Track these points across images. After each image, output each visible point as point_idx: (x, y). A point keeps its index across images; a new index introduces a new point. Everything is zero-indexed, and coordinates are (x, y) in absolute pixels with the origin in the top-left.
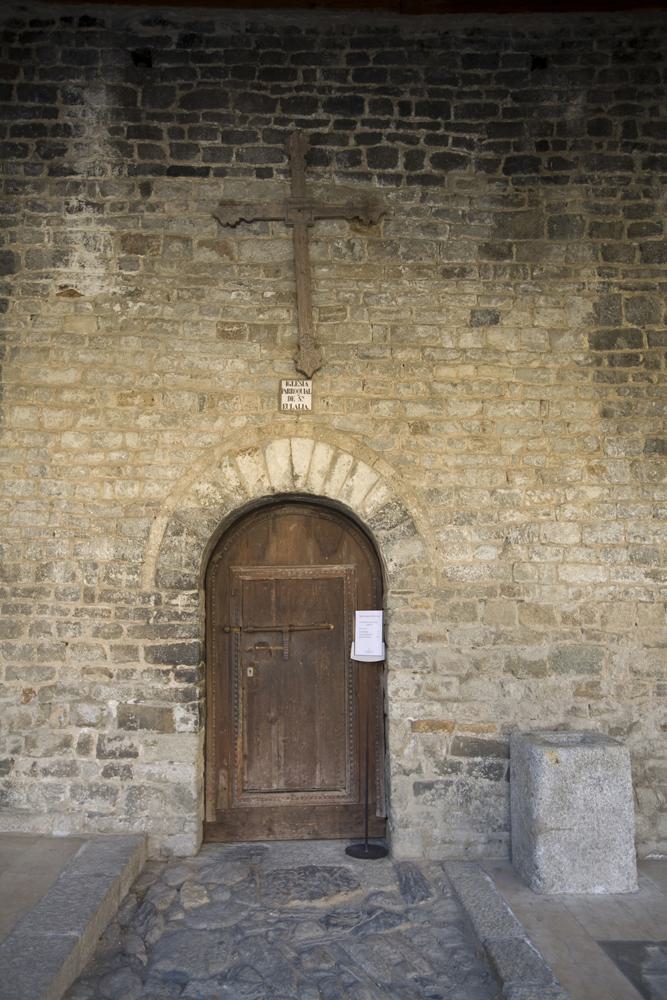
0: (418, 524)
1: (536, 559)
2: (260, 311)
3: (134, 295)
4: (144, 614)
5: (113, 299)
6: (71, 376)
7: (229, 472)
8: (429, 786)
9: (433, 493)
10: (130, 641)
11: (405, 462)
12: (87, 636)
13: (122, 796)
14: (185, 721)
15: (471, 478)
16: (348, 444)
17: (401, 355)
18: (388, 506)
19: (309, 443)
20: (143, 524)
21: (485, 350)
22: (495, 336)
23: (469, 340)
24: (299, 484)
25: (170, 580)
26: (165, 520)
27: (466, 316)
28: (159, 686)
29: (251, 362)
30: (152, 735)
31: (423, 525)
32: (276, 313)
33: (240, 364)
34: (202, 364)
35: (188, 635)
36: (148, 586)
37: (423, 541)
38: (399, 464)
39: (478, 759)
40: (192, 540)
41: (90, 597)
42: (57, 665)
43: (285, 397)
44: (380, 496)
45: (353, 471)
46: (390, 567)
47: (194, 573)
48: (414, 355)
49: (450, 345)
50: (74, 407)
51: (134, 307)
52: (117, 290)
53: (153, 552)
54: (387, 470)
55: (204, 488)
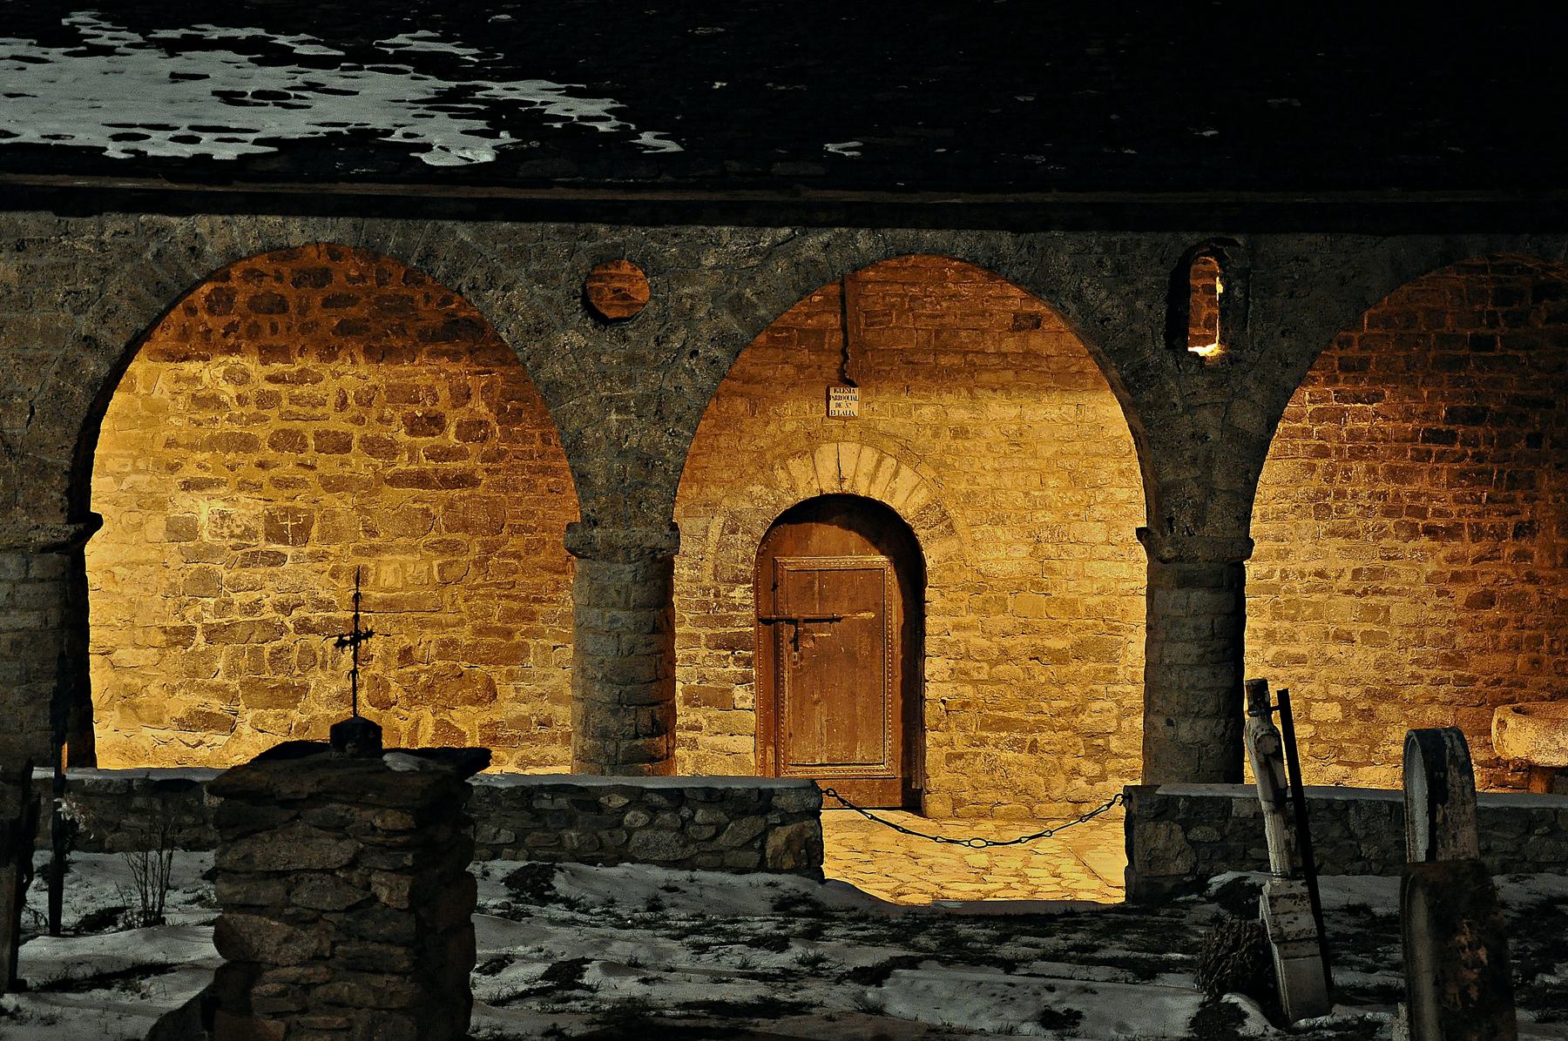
0: (955, 524)
1: (1064, 556)
2: (808, 316)
7: (781, 474)
8: (960, 756)
9: (969, 497)
10: (693, 630)
11: (945, 465)
14: (743, 699)
15: (1007, 480)
16: (893, 448)
17: (943, 361)
18: (928, 506)
19: (855, 447)
20: (701, 523)
21: (1027, 354)
22: (1036, 341)
23: (1010, 344)
24: (846, 487)
25: (728, 575)
26: (722, 520)
27: (1009, 320)
29: (800, 368)
31: (960, 525)
32: (825, 318)
34: (752, 370)
35: (743, 624)
37: (960, 539)
38: (939, 466)
39: (1004, 734)
40: (747, 538)
43: (832, 403)
44: (921, 497)
45: (896, 474)
46: (929, 563)
47: (748, 569)
48: (956, 360)
49: (992, 350)
54: (929, 473)
55: (757, 489)
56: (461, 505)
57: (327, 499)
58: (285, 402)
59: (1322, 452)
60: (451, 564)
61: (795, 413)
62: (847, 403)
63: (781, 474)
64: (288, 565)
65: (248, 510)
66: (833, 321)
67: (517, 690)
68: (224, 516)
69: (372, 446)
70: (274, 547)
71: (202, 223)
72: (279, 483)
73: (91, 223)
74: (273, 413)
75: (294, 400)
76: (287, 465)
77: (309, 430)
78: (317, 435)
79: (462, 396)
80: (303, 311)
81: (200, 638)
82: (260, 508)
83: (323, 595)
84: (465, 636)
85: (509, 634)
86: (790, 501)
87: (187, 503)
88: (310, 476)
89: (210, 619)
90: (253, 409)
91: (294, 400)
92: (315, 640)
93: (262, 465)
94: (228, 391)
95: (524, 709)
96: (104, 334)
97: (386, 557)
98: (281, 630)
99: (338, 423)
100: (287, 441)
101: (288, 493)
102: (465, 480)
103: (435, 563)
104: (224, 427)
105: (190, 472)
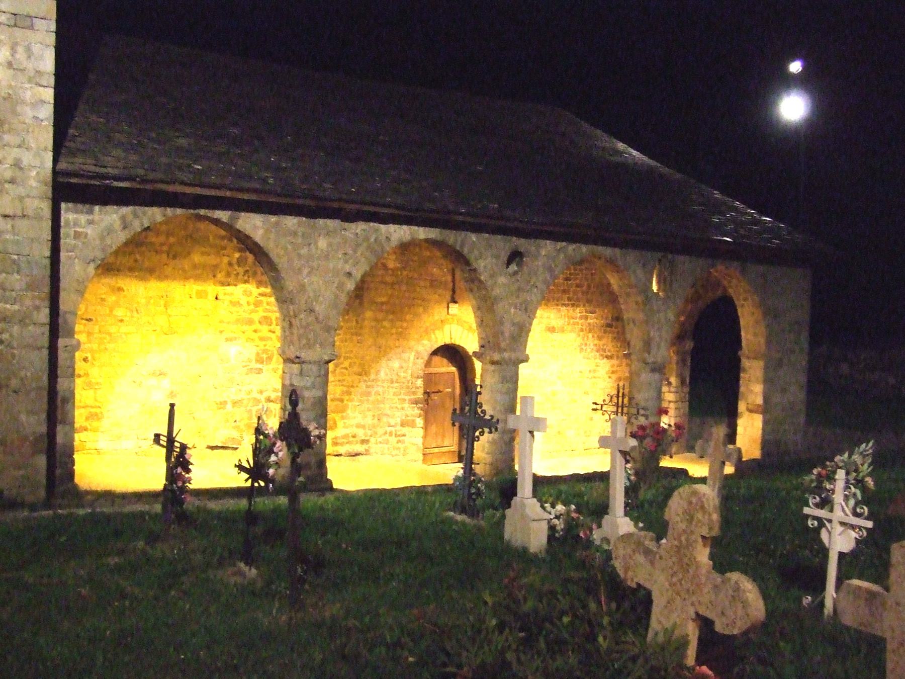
3: (404, 268)
4: (408, 387)
5: (397, 269)
6: (384, 300)
12: (391, 396)
13: (402, 450)
25: (416, 375)
30: (410, 429)
33: (437, 296)
35: (420, 395)
36: (409, 378)
41: (392, 382)
42: (382, 406)
50: (387, 312)
51: (405, 273)
53: (411, 365)
58: (265, 304)
59: (582, 330)
61: (438, 312)
62: (454, 308)
63: (433, 336)
66: (449, 278)
71: (392, 228)
73: (353, 226)
74: (260, 309)
75: (268, 304)
76: (265, 329)
82: (254, 350)
86: (436, 346)
90: (252, 307)
92: (271, 405)
93: (255, 331)
94: (244, 300)
95: (348, 431)
96: (354, 272)
98: (259, 401)
101: (264, 343)
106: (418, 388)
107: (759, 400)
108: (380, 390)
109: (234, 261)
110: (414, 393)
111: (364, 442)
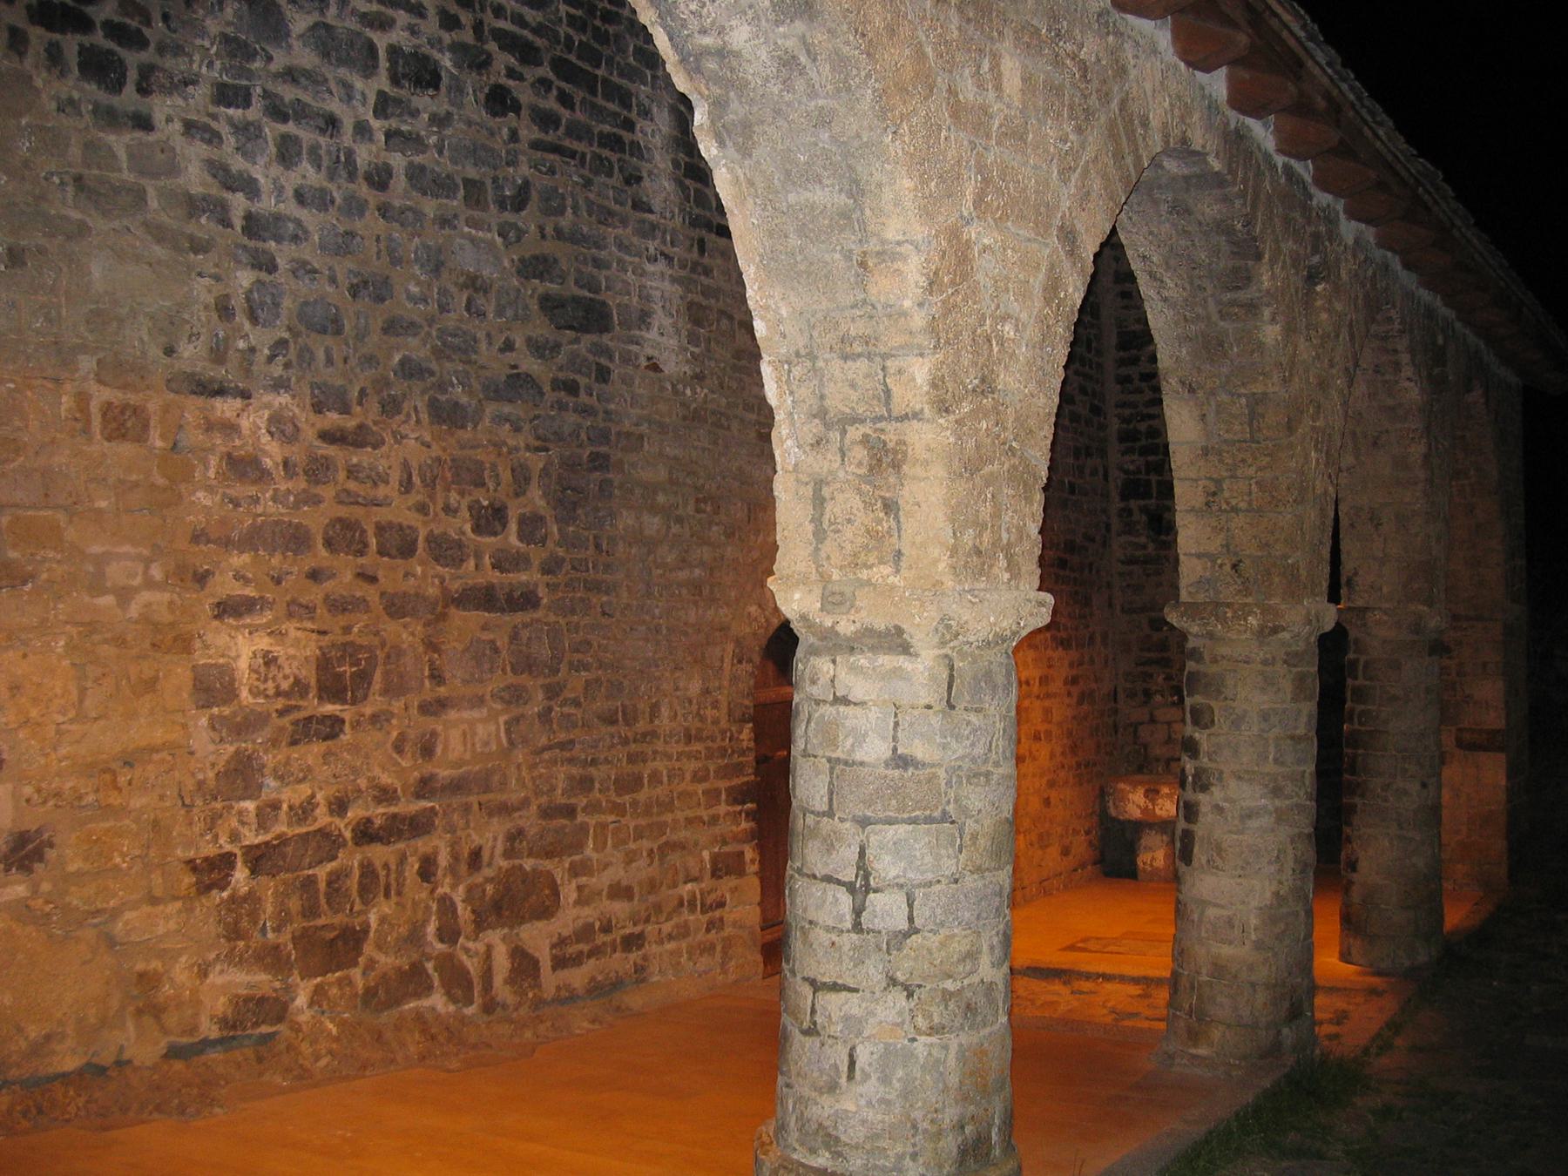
14: (753, 861)
20: (717, 651)
28: (734, 828)
36: (724, 724)
40: (749, 668)
41: (689, 738)
52: (686, 368)
56: (525, 634)
57: (391, 628)
58: (342, 475)
60: (517, 720)
64: (347, 736)
65: (298, 650)
67: (580, 888)
68: (270, 660)
69: (446, 551)
70: (330, 708)
72: (339, 606)
74: (327, 492)
76: (344, 569)
77: (369, 520)
78: (380, 529)
79: (521, 478)
80: (361, 336)
81: (240, 874)
83: (386, 779)
84: (529, 821)
85: (570, 812)
87: (222, 640)
88: (371, 593)
89: (251, 838)
91: (352, 472)
93: (315, 575)
95: (589, 914)
97: (452, 714)
99: (400, 511)
100: (344, 536)
101: (342, 620)
102: (525, 600)
103: (502, 720)
104: (269, 508)
105: (225, 586)
106: (743, 753)
107: (1494, 719)
108: (660, 765)
109: (238, 302)
110: (738, 769)
111: (632, 942)
